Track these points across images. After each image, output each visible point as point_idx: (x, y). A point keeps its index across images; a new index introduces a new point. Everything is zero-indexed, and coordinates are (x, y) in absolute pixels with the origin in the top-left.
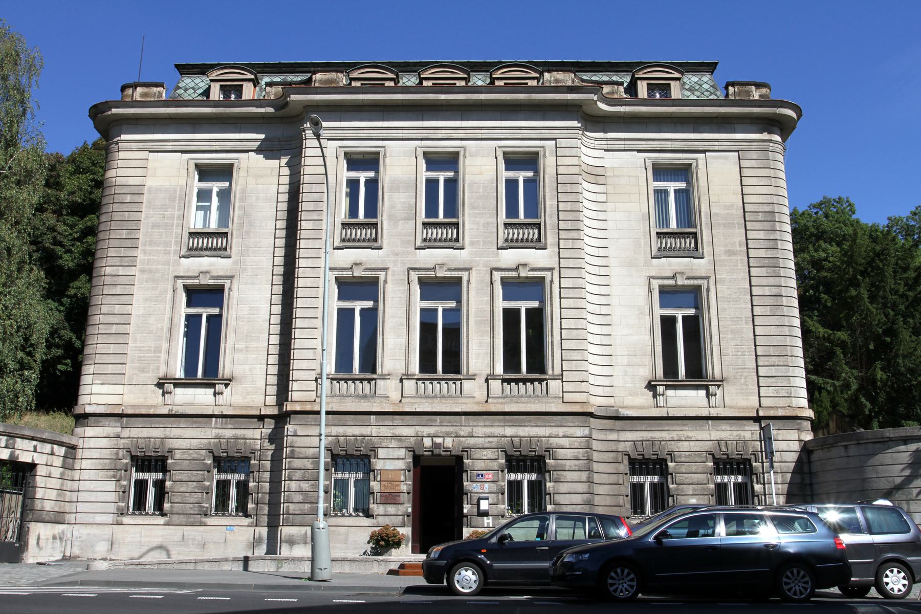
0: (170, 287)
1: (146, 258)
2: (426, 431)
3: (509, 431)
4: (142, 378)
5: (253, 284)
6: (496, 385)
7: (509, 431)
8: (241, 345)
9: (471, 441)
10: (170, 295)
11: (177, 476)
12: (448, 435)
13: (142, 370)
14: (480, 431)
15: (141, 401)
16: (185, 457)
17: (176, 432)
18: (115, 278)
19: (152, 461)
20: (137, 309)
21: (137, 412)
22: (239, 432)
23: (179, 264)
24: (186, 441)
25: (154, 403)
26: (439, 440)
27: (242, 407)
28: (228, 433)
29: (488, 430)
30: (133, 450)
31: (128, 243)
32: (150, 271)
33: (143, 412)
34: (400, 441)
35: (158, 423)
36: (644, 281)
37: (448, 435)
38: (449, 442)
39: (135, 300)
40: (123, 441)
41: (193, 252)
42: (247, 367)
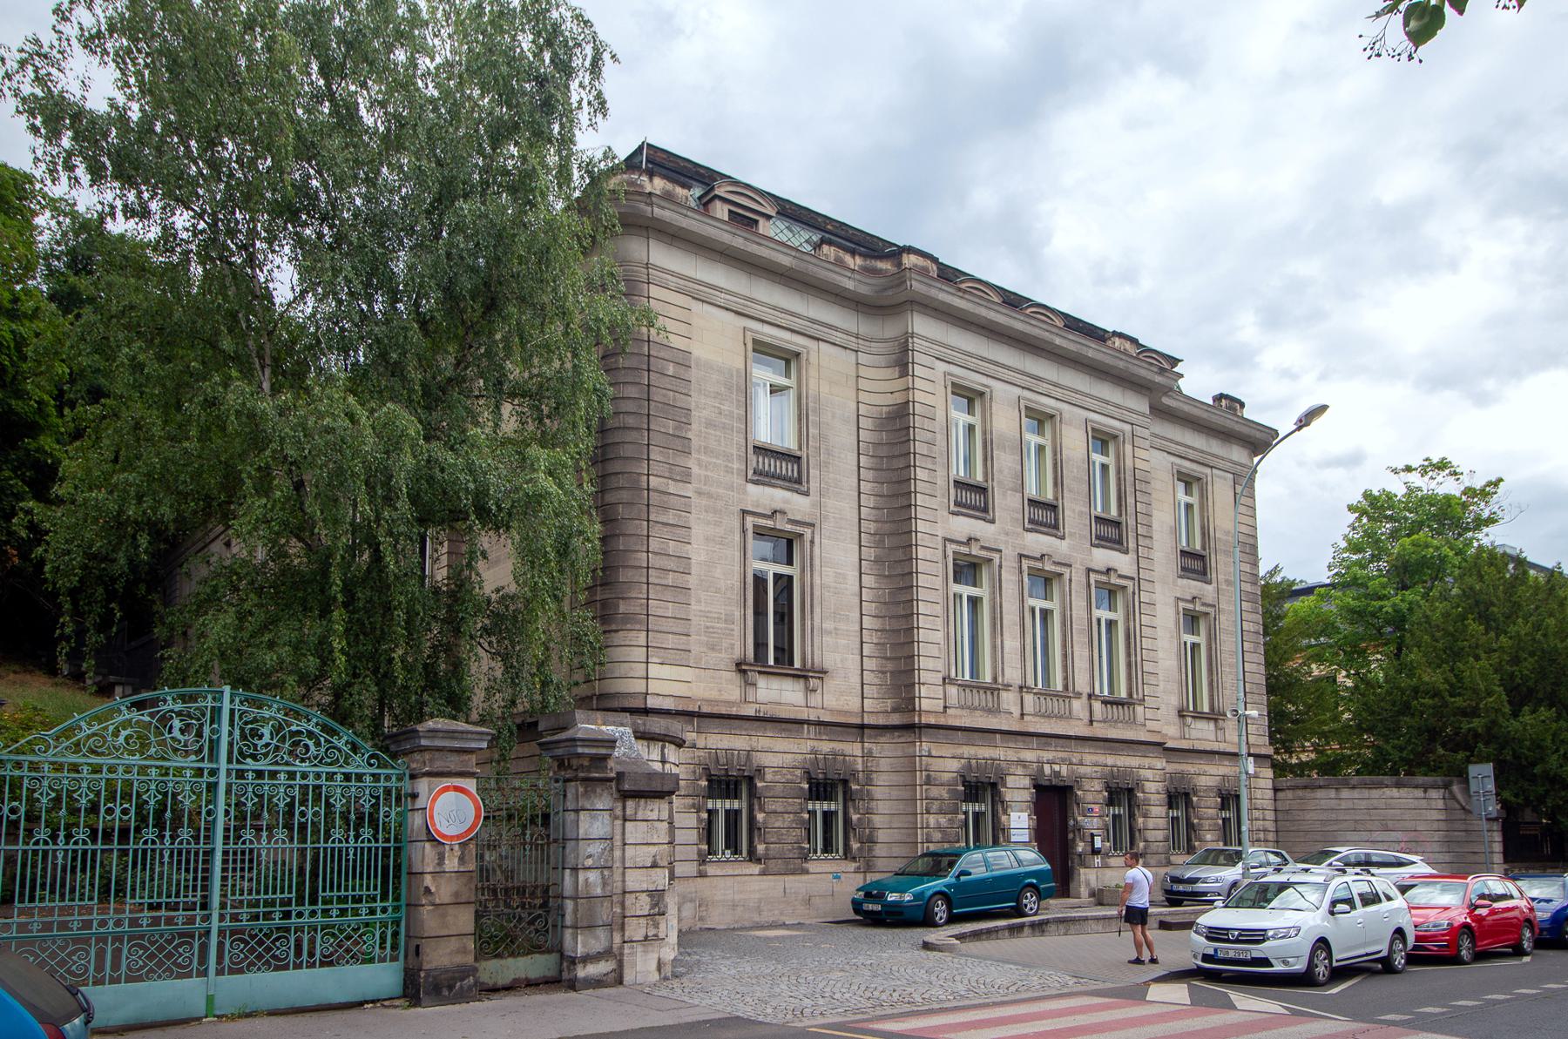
0: (737, 524)
1: (703, 473)
2: (1047, 755)
3: (1110, 760)
4: (712, 658)
5: (837, 539)
6: (1097, 705)
7: (1110, 760)
8: (828, 625)
9: (1082, 770)
10: (737, 537)
11: (771, 805)
12: (1063, 761)
13: (713, 648)
14: (1088, 759)
15: (713, 694)
16: (778, 778)
17: (763, 742)
18: (665, 498)
19: (729, 781)
20: (698, 552)
21: (715, 710)
22: (838, 746)
23: (745, 492)
24: (779, 756)
25: (725, 697)
26: (1057, 768)
27: (840, 712)
28: (826, 747)
29: (1095, 758)
30: (712, 767)
31: (678, 444)
32: (709, 495)
33: (723, 711)
34: (1025, 767)
35: (740, 728)
36: (1172, 600)
37: (1063, 761)
38: (1064, 770)
39: (698, 532)
40: (698, 753)
41: (763, 477)
42: (838, 657)
